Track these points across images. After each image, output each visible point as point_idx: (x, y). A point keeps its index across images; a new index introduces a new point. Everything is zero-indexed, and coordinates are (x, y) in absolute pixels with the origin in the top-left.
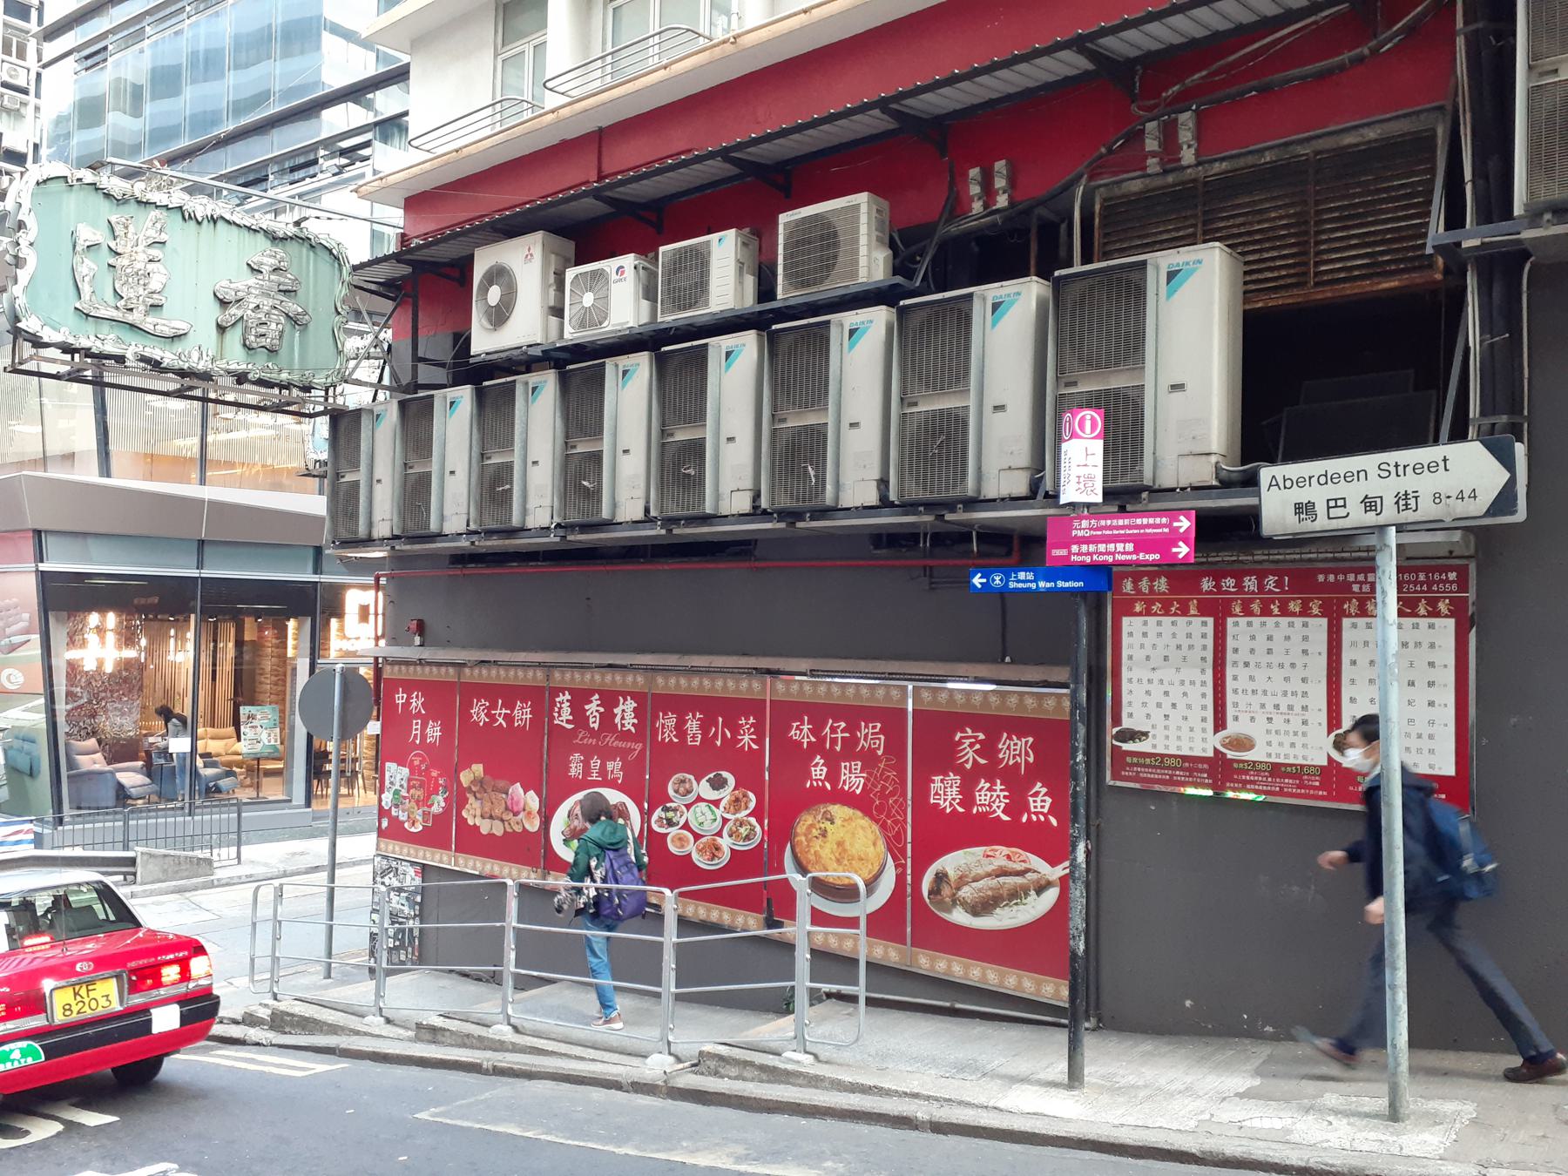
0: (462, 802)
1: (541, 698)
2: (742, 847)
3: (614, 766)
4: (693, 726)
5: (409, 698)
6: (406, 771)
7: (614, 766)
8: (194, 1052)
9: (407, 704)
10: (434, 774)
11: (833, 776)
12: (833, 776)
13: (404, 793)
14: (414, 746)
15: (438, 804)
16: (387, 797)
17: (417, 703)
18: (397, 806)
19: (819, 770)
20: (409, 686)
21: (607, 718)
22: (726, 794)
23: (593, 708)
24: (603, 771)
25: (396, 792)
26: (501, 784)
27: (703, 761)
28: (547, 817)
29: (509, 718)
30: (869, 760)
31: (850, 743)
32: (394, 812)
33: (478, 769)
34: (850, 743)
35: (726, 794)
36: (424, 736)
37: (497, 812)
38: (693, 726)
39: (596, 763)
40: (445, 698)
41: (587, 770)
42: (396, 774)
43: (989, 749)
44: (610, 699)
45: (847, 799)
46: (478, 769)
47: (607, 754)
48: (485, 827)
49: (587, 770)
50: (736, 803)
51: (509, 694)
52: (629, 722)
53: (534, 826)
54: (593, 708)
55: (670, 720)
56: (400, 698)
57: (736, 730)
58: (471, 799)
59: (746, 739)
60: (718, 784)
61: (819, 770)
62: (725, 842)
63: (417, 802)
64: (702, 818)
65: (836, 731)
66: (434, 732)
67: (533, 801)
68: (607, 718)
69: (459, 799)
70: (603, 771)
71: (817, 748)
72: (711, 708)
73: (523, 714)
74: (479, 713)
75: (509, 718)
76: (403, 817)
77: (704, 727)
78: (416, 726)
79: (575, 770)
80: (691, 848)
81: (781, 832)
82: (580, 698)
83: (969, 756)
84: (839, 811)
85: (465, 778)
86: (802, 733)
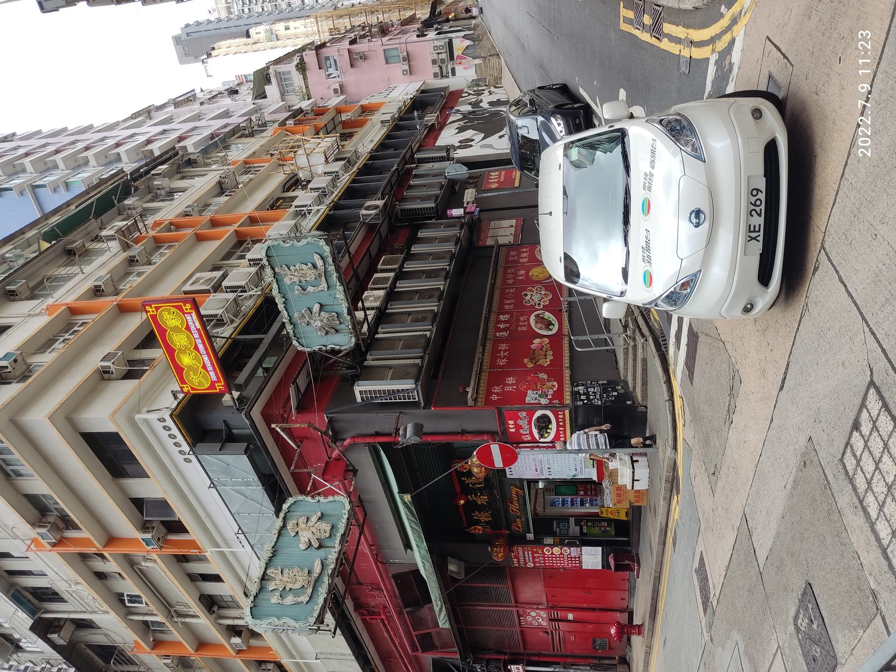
1: (498, 341)
3: (522, 319)
4: (508, 302)
5: (494, 393)
6: (529, 392)
7: (522, 319)
8: (675, 364)
9: (497, 394)
13: (540, 392)
14: (517, 389)
15: (543, 376)
16: (544, 401)
17: (497, 389)
18: (547, 396)
19: (521, 278)
20: (489, 393)
21: (505, 322)
22: (529, 293)
23: (502, 326)
25: (540, 396)
26: (531, 352)
27: (519, 298)
32: (550, 397)
33: (526, 361)
35: (529, 293)
36: (513, 385)
38: (508, 302)
39: (521, 324)
40: (497, 378)
42: (531, 397)
44: (500, 322)
45: (527, 273)
46: (526, 361)
47: (518, 321)
48: (550, 358)
49: (524, 326)
51: (495, 351)
52: (507, 316)
53: (546, 340)
54: (502, 326)
56: (494, 397)
57: (509, 293)
60: (526, 295)
62: (543, 292)
63: (543, 385)
64: (536, 298)
66: (511, 380)
68: (505, 322)
69: (542, 369)
72: (503, 296)
73: (503, 346)
76: (551, 392)
81: (539, 282)
82: (499, 330)
84: (531, 274)
86: (511, 281)
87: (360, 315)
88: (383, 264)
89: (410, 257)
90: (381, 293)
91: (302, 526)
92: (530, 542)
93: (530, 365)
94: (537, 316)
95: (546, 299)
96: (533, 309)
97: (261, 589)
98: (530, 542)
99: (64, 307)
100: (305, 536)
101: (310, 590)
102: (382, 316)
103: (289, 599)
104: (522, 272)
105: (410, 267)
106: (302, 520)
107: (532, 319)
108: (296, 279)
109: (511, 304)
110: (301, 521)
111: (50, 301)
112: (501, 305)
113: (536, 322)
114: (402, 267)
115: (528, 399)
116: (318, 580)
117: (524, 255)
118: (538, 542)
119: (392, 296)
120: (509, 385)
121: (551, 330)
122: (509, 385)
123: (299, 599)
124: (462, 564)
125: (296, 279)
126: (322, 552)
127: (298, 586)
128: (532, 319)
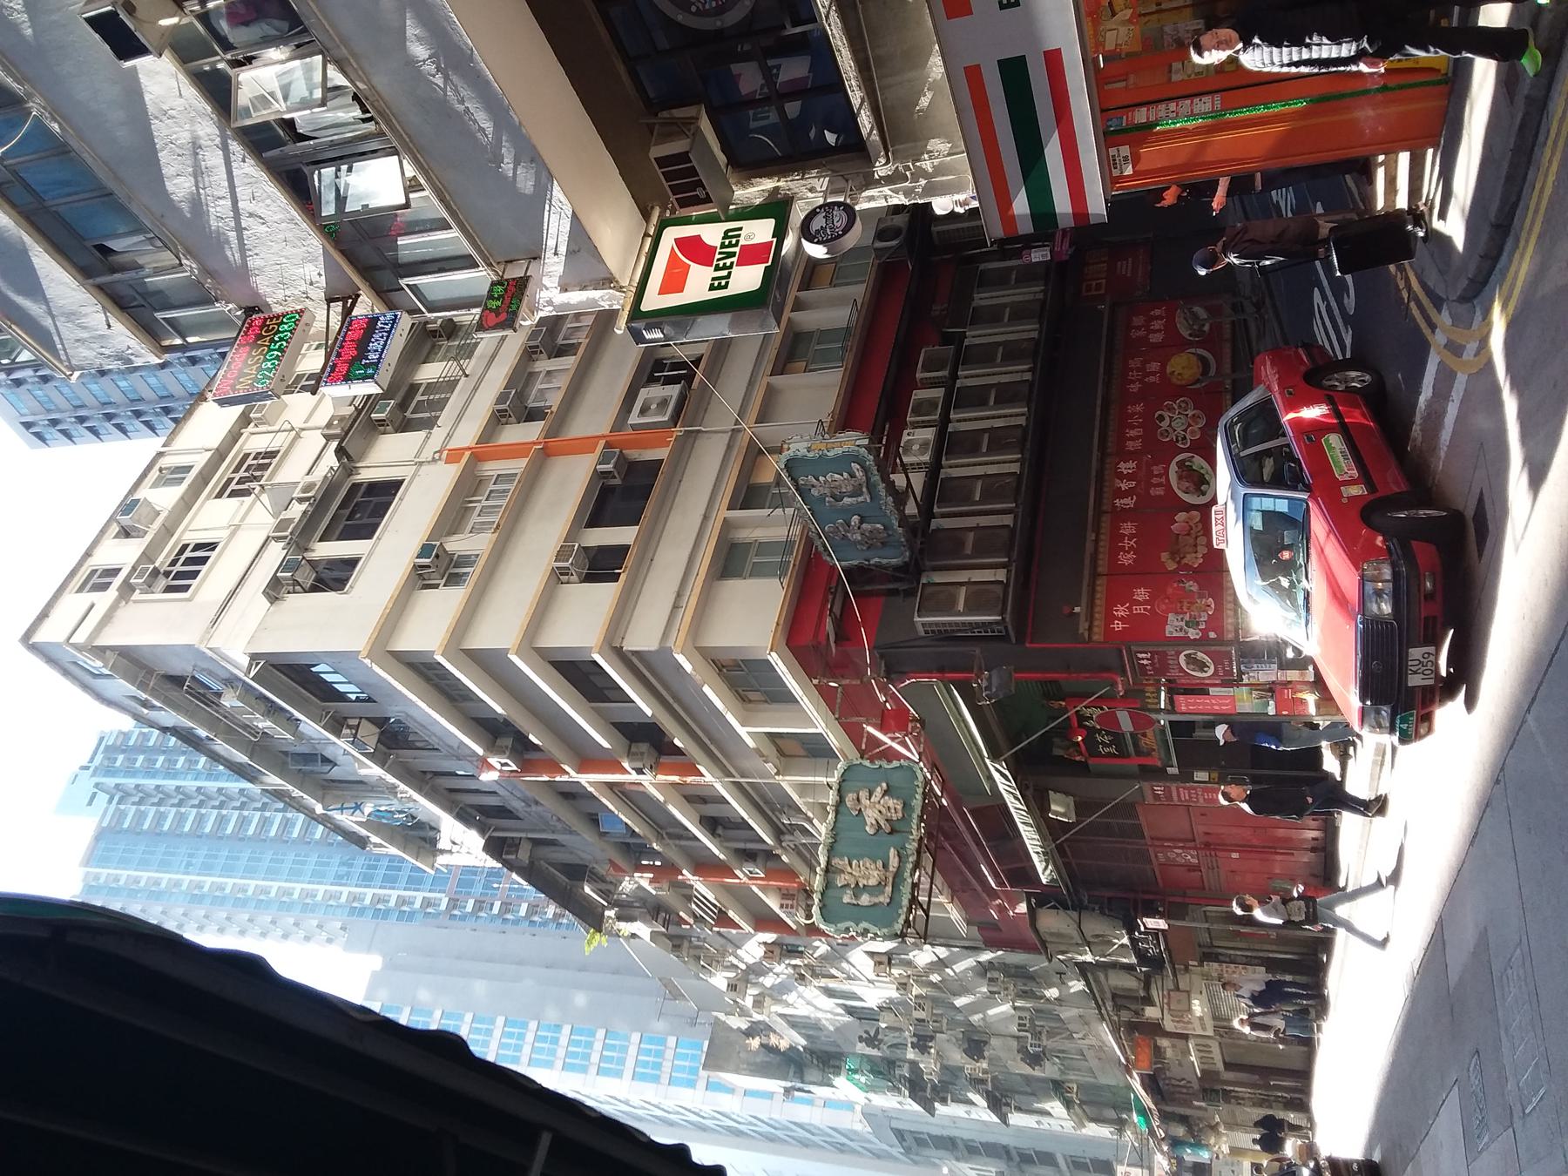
0: (1188, 567)
2: (1191, 405)
4: (1132, 433)
6: (1171, 617)
7: (1157, 470)
9: (1122, 619)
10: (1170, 591)
11: (1153, 374)
12: (1153, 374)
13: (1187, 617)
14: (1152, 611)
15: (1192, 586)
17: (1121, 611)
19: (1152, 379)
20: (1110, 618)
21: (1129, 477)
22: (1166, 414)
24: (1159, 476)
27: (1150, 425)
28: (1189, 507)
29: (1131, 537)
30: (1145, 363)
31: (1138, 370)
33: (1165, 556)
34: (1138, 370)
35: (1166, 414)
36: (1146, 602)
37: (1191, 541)
38: (1132, 433)
39: (1155, 481)
41: (1158, 485)
43: (1138, 328)
44: (1121, 476)
45: (1163, 366)
47: (1151, 475)
49: (1158, 485)
50: (1170, 409)
51: (1116, 537)
52: (1131, 464)
54: (1124, 486)
55: (1129, 443)
56: (1118, 626)
58: (1185, 561)
59: (1138, 408)
60: (1161, 418)
61: (1152, 379)
64: (1179, 426)
65: (1133, 375)
66: (1141, 594)
67: (1181, 516)
68: (1129, 477)
70: (1159, 476)
71: (1141, 381)
73: (1128, 528)
74: (1126, 559)
75: (1131, 537)
76: (1204, 618)
77: (1133, 428)
78: (1138, 610)
79: (1160, 491)
80: (1196, 427)
83: (1142, 333)
84: (1169, 370)
85: (1171, 566)
86: (1135, 387)
87: (899, 480)
88: (926, 369)
89: (965, 356)
90: (929, 434)
91: (865, 802)
92: (1173, 778)
93: (1171, 566)
94: (1181, 464)
95: (1196, 427)
96: (1173, 449)
97: (828, 884)
98: (1173, 778)
99: (468, 454)
100: (871, 816)
101: (889, 889)
102: (938, 489)
103: (865, 900)
104: (1154, 366)
105: (969, 378)
106: (863, 794)
107: (1173, 468)
108: (827, 491)
109: (1138, 437)
110: (863, 794)
111: (438, 434)
112: (1122, 439)
113: (1180, 478)
114: (954, 376)
115: (1170, 631)
116: (898, 875)
117: (1157, 325)
118: (1185, 777)
119: (947, 444)
120: (1139, 603)
121: (1204, 494)
122: (1139, 603)
123: (876, 900)
124: (1071, 800)
125: (827, 491)
126: (896, 838)
127: (873, 882)
128: (1173, 468)
